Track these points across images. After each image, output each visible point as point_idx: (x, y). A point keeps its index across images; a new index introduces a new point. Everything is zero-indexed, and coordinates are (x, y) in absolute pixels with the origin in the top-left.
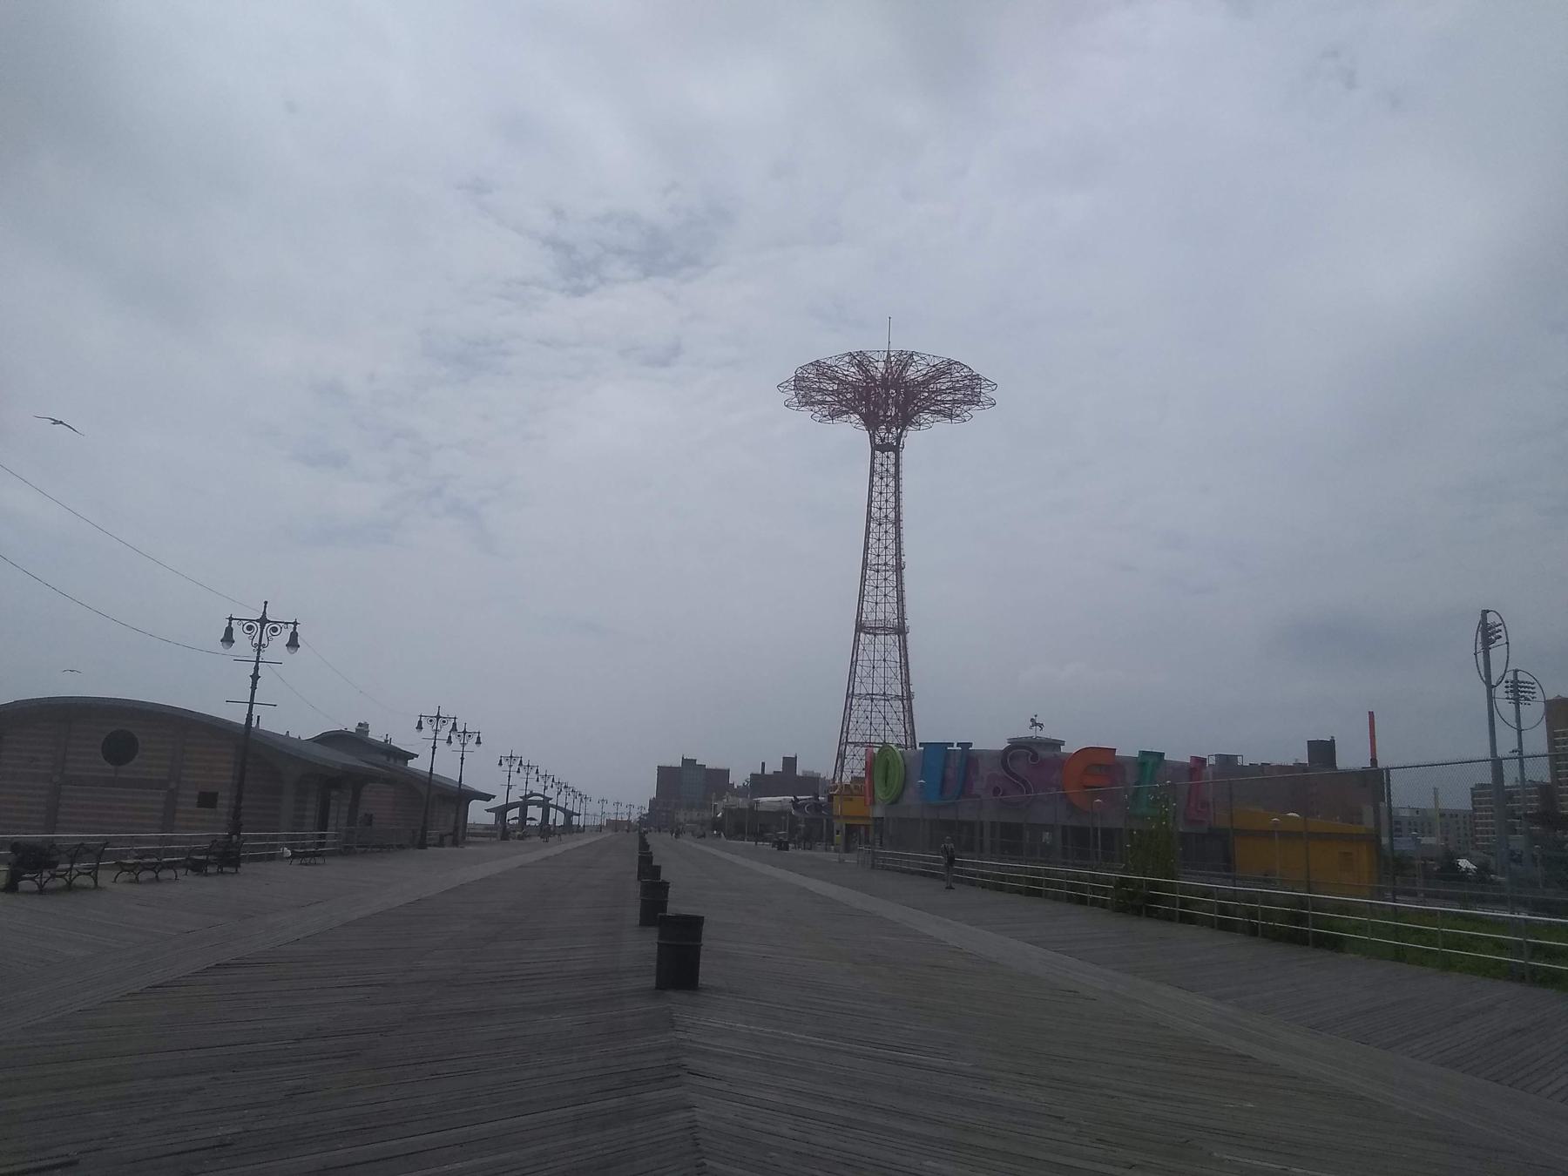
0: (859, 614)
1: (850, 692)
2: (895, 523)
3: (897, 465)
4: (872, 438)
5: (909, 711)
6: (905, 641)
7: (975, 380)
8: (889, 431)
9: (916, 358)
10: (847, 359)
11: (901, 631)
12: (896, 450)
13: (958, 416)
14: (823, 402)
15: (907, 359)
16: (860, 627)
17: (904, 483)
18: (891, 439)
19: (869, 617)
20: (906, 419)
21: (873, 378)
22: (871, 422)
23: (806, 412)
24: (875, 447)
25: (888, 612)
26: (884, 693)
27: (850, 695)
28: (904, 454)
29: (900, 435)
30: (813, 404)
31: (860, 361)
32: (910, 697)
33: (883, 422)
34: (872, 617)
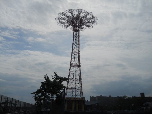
3: (79, 34)
6: (80, 68)
7: (93, 18)
9: (82, 11)
11: (79, 66)
12: (78, 31)
15: (80, 11)
16: (71, 65)
19: (73, 63)
20: (80, 27)
21: (74, 17)
22: (74, 27)
26: (76, 78)
31: (71, 11)
32: (81, 79)
34: (73, 63)
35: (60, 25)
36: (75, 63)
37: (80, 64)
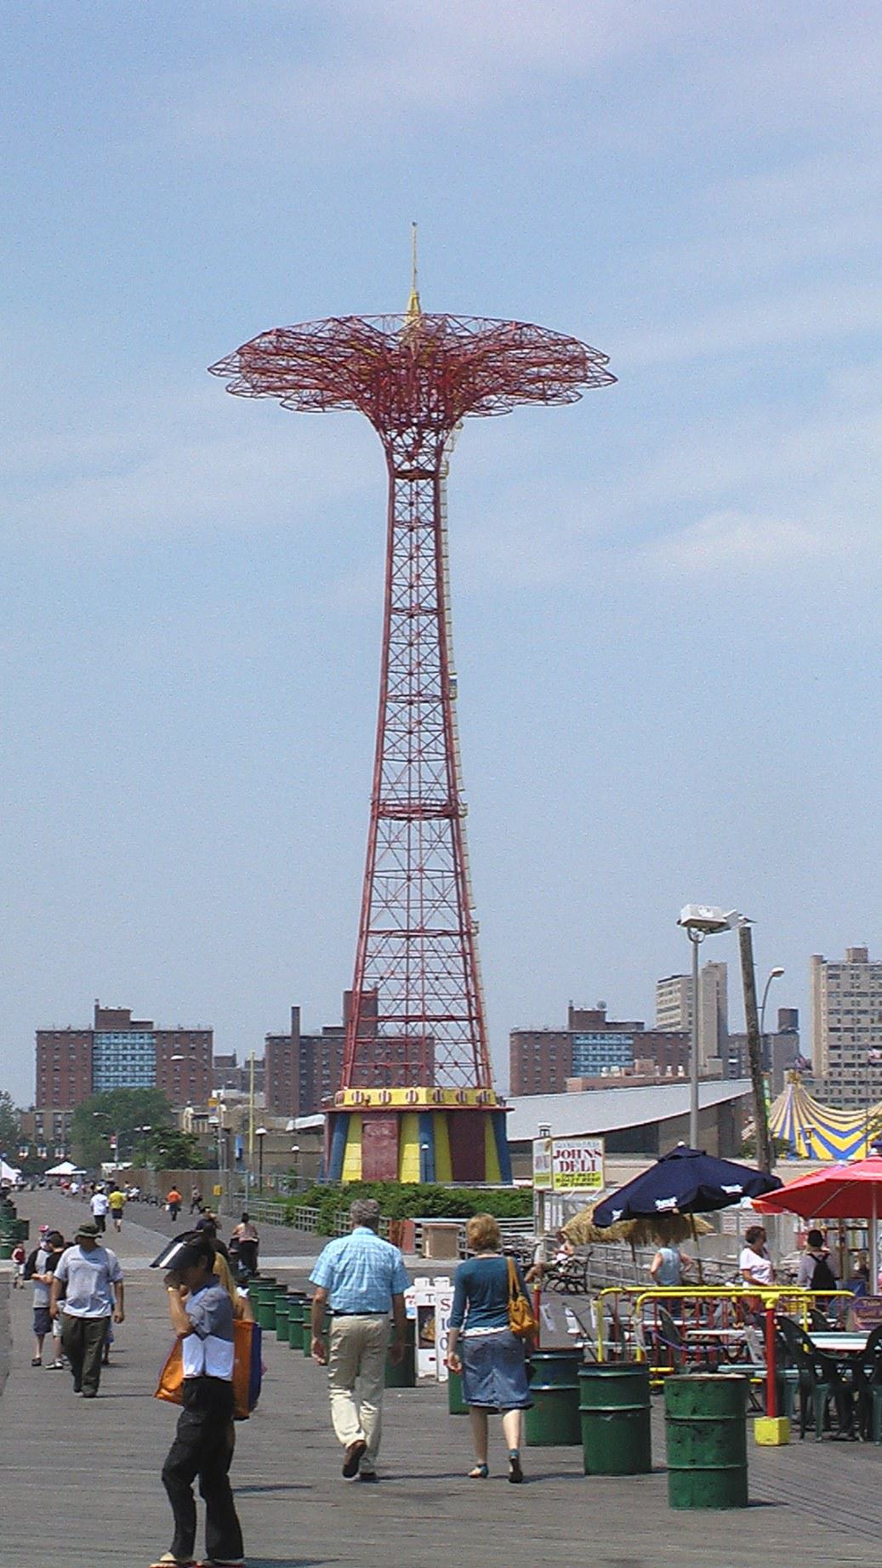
0: (377, 788)
1: (365, 929)
2: (437, 615)
4: (390, 450)
5: (468, 955)
8: (418, 444)
10: (330, 325)
11: (451, 811)
12: (434, 476)
13: (554, 396)
14: (298, 386)
16: (379, 811)
17: (451, 538)
18: (425, 461)
23: (271, 402)
24: (396, 473)
25: (429, 781)
27: (365, 933)
28: (449, 484)
29: (438, 451)
30: (281, 388)
33: (409, 425)
35: (263, 394)
36: (415, 786)
37: (453, 798)
